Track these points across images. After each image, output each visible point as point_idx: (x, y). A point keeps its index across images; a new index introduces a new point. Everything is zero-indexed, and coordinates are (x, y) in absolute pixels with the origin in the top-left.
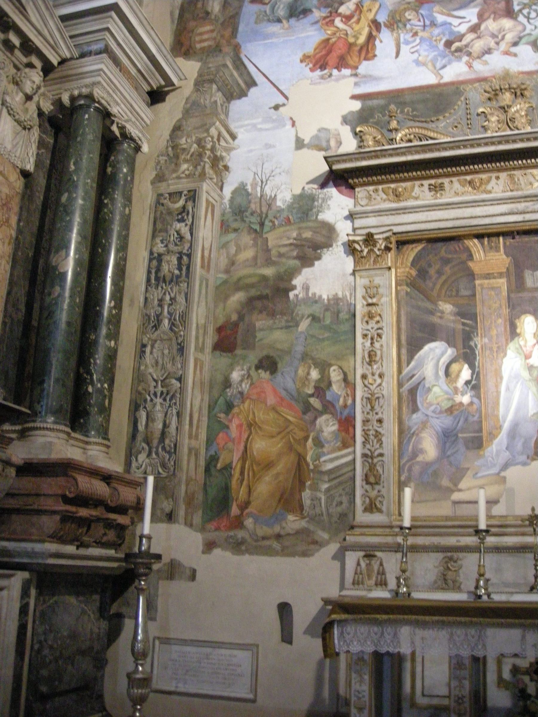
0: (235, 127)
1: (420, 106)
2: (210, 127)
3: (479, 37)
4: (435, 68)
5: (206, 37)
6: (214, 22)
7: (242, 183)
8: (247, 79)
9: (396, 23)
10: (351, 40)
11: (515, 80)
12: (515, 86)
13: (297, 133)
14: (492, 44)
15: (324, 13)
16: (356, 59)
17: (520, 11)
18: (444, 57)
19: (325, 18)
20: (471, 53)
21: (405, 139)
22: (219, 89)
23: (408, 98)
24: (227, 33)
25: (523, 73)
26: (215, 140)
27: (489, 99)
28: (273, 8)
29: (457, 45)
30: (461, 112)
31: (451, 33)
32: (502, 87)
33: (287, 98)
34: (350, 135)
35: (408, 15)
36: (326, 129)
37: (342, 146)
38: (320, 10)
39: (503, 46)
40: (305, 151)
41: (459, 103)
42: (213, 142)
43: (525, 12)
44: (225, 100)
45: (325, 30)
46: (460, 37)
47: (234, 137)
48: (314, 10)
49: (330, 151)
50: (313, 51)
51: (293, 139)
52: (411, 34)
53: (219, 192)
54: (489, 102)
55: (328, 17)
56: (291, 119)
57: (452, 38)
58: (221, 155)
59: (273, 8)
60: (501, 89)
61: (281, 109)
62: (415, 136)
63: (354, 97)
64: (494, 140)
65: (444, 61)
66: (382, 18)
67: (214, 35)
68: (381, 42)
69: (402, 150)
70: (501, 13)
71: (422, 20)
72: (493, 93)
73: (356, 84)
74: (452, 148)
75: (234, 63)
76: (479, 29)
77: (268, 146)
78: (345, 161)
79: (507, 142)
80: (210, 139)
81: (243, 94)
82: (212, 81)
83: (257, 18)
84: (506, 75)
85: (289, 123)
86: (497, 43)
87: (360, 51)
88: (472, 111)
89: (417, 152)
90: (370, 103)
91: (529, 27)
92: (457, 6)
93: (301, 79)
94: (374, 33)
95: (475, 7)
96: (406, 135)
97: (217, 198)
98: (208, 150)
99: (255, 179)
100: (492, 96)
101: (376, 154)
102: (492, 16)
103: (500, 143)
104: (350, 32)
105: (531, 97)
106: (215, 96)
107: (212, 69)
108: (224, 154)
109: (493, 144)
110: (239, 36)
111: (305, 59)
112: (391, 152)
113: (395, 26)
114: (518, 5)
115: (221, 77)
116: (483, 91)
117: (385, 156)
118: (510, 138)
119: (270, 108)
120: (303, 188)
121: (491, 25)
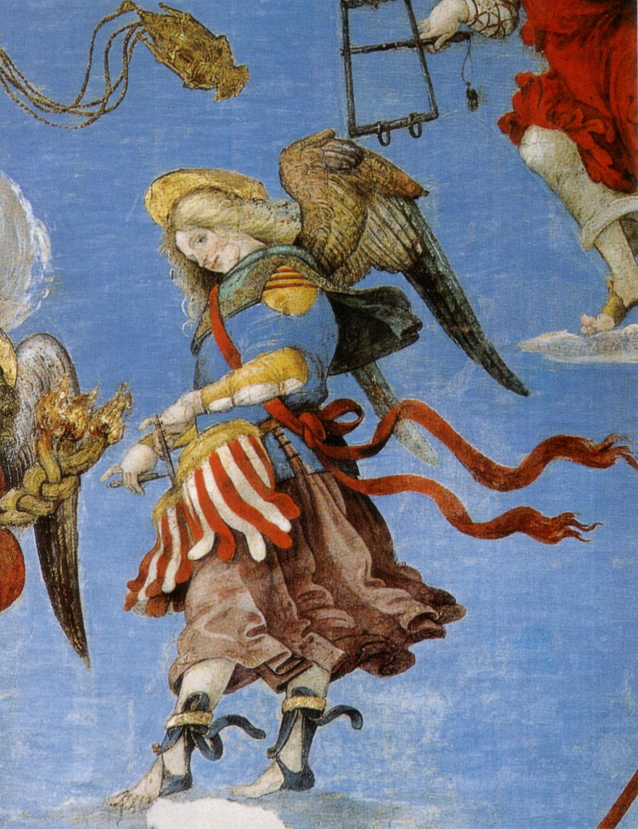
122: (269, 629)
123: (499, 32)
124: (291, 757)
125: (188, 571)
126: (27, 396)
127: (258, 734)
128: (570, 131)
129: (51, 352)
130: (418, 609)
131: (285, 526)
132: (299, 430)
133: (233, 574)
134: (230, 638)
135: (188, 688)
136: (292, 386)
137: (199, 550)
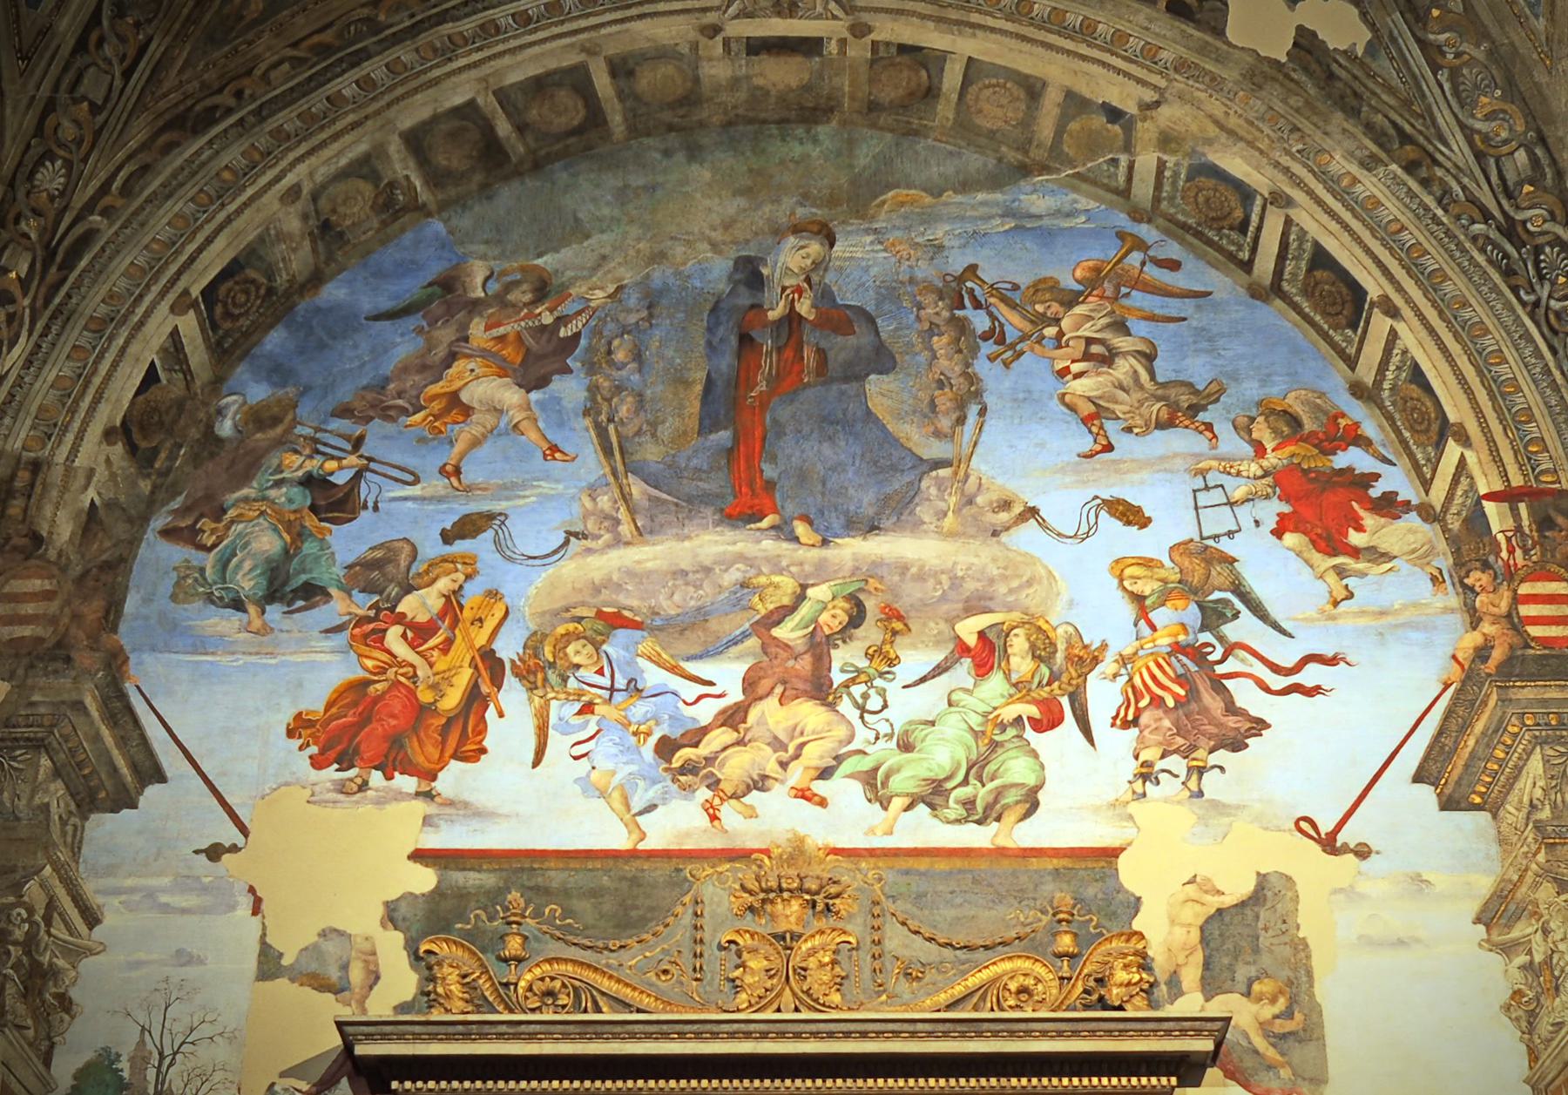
0: (97, 892)
1: (583, 906)
2: (27, 878)
3: (740, 742)
4: (628, 808)
5: (29, 609)
6: (55, 571)
7: (107, 1050)
8: (140, 757)
9: (543, 669)
10: (425, 696)
11: (816, 870)
12: (814, 887)
13: (264, 935)
14: (772, 768)
15: (362, 603)
16: (434, 753)
17: (846, 685)
18: (654, 782)
19: (361, 621)
20: (718, 781)
21: (536, 988)
22: (57, 773)
23: (556, 877)
24: (92, 610)
25: (836, 851)
26: (38, 918)
27: (751, 909)
28: (224, 564)
29: (686, 753)
30: (680, 932)
31: (675, 719)
32: (784, 885)
33: (244, 831)
34: (403, 958)
35: (577, 652)
36: (341, 933)
37: (380, 983)
38: (350, 595)
39: (797, 775)
40: (282, 983)
41: (679, 909)
42: (33, 923)
43: (857, 690)
44: (73, 807)
45: (360, 655)
46: (697, 736)
47: (92, 918)
48: (333, 591)
49: (346, 994)
50: (321, 707)
51: (255, 948)
52: (577, 706)
53: (41, 1067)
54: (749, 916)
55: (369, 620)
56: (252, 890)
57: (676, 734)
58: (51, 964)
59: (224, 564)
60: (781, 890)
61: (226, 857)
62: (564, 985)
63: (419, 856)
64: (752, 1027)
65: (652, 794)
66: (508, 648)
67: (53, 607)
68: (501, 715)
69: (532, 1028)
70: (801, 686)
71: (607, 671)
72: (762, 895)
73: (427, 821)
74: (648, 1036)
75: (105, 703)
76: (744, 721)
77: (185, 958)
78: (385, 1037)
79: (781, 1035)
80: (24, 914)
81: (125, 800)
82: (38, 745)
83: (177, 584)
84: (797, 852)
85: (246, 902)
86: (784, 765)
87: (445, 730)
88: (707, 936)
89: (566, 1037)
90: (458, 877)
91: (862, 736)
92: (697, 650)
93: (287, 784)
94: (485, 688)
95: (739, 657)
96: (542, 979)
97: (32, 1083)
98: (15, 943)
99: (142, 1042)
100: (756, 905)
101: (467, 1031)
102: (779, 690)
103: (764, 1036)
104: (419, 673)
105: (851, 916)
106: (46, 791)
107: (42, 710)
108: (61, 963)
109: (748, 1035)
110: (123, 628)
111: (299, 726)
112: (503, 1028)
113: (540, 676)
114: (843, 671)
115: (66, 739)
116: (737, 886)
117: (483, 1036)
118: (791, 1027)
119: (197, 852)
120: (273, 1084)
121: (770, 714)
122: (1178, 734)
123: (1267, 497)
124: (1193, 784)
125: (1138, 712)
126: (1061, 646)
127: (1177, 776)
128: (1305, 533)
129: (1071, 629)
130: (1248, 725)
131: (1182, 692)
132: (1186, 655)
133: (1160, 713)
134: (1160, 738)
135: (1142, 758)
136: (1181, 638)
137: (1143, 703)
